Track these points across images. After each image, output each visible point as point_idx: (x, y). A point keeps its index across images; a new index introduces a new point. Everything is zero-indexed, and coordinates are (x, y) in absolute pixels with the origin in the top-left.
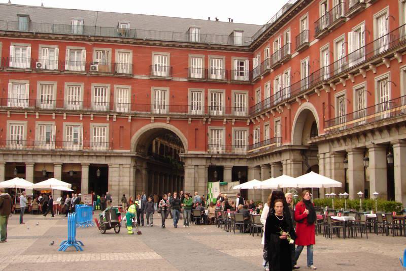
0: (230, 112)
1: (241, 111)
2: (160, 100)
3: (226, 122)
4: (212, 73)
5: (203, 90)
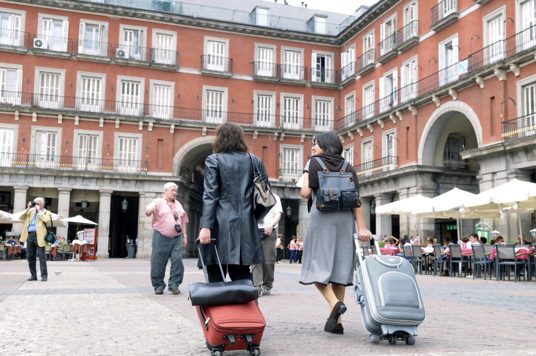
0: (310, 126)
1: (324, 124)
3: (305, 139)
4: (286, 71)
5: (274, 94)
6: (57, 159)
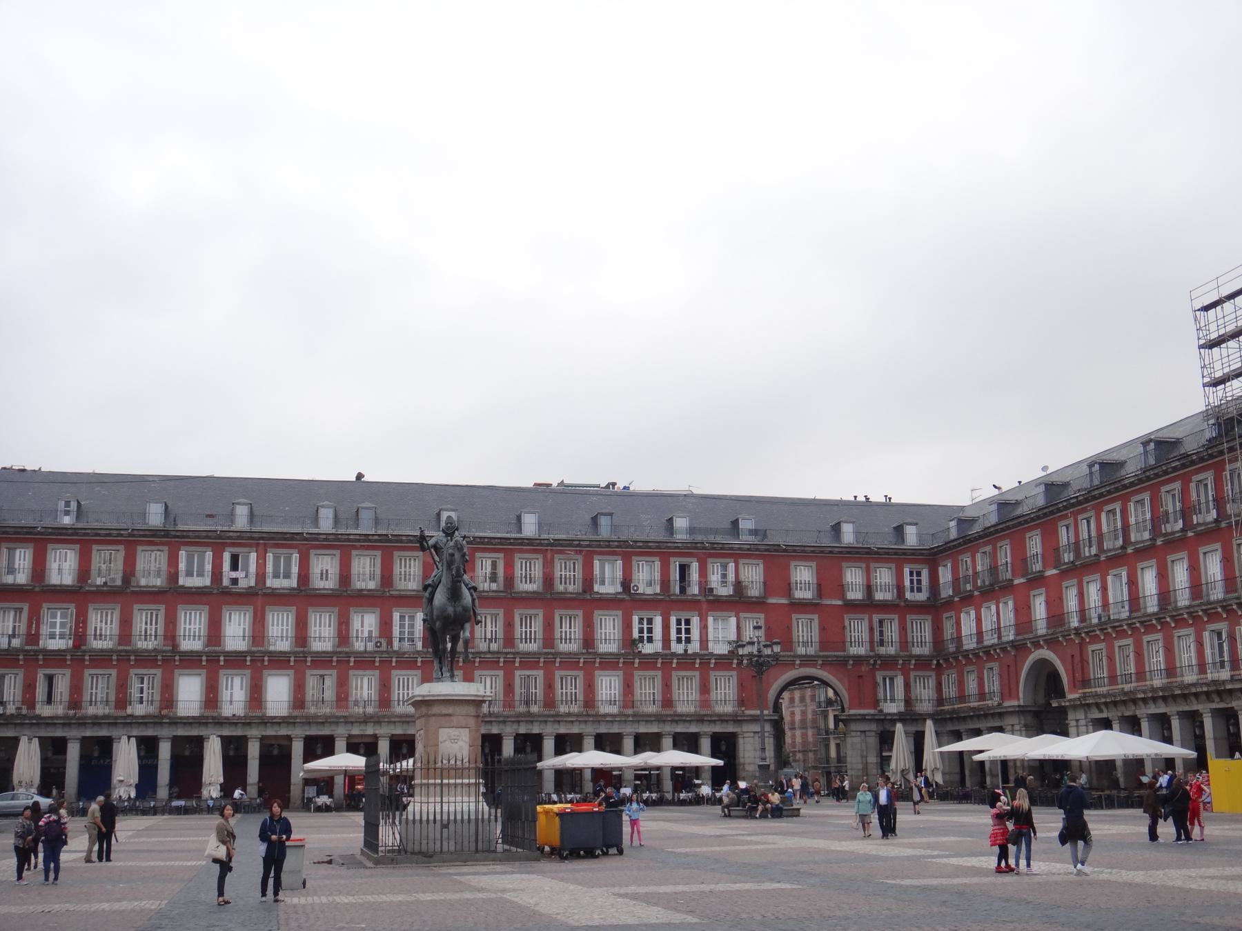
2: (806, 632)
5: (866, 617)
6: (659, 703)
